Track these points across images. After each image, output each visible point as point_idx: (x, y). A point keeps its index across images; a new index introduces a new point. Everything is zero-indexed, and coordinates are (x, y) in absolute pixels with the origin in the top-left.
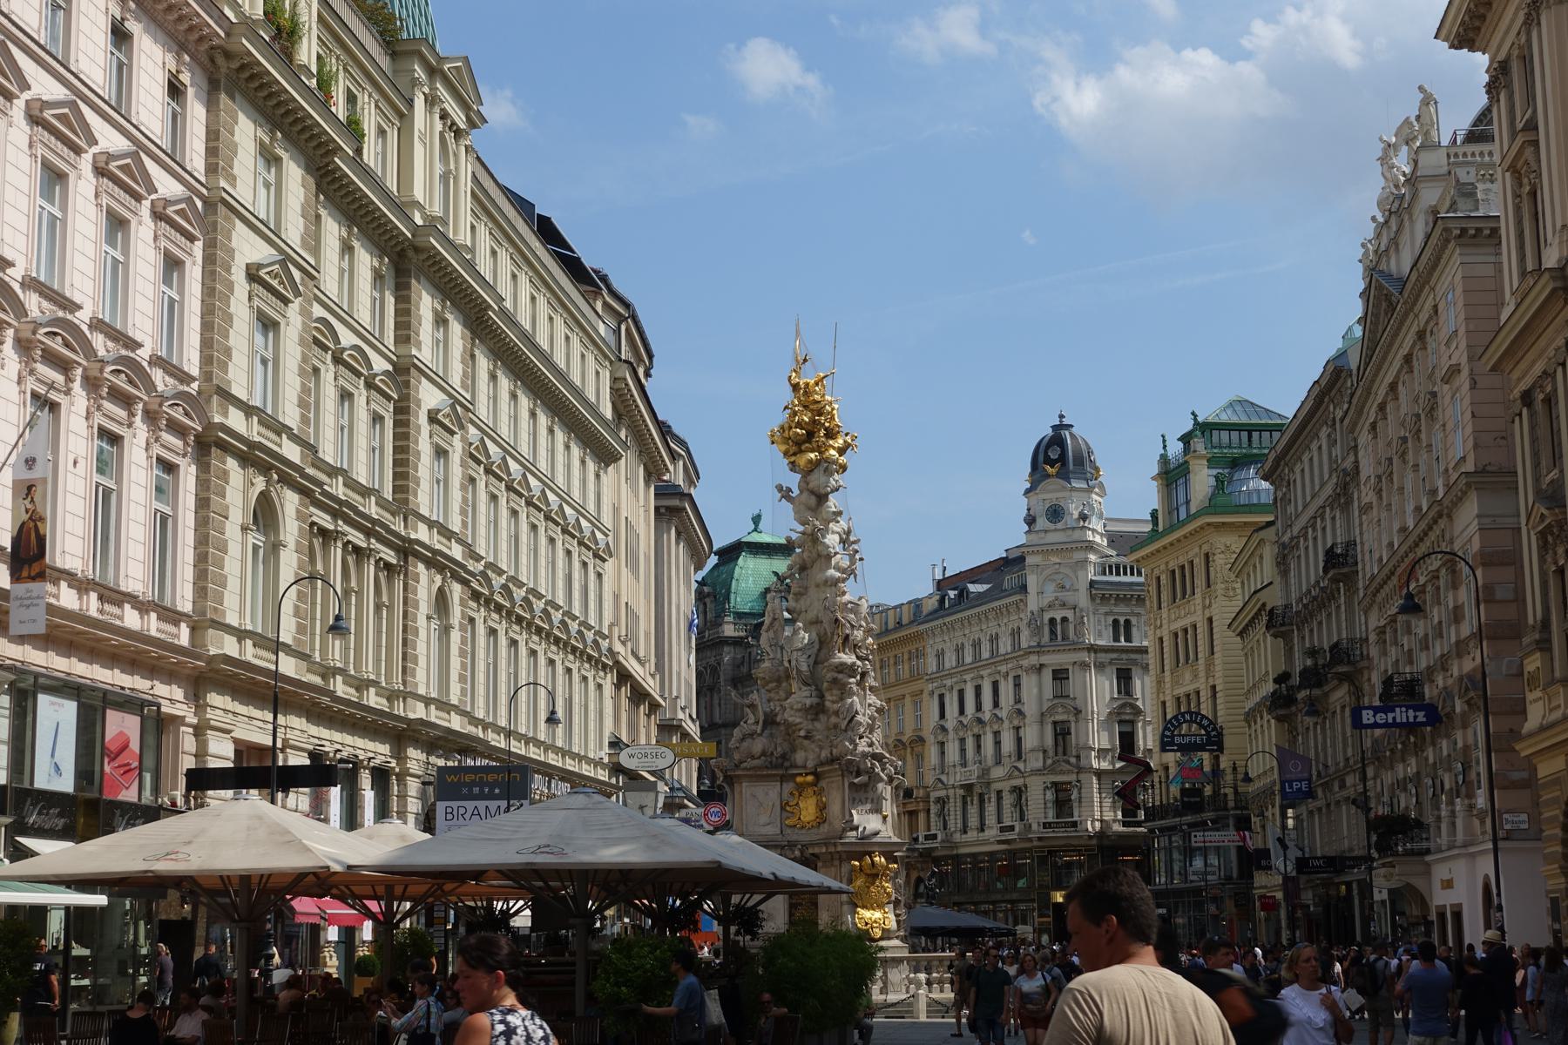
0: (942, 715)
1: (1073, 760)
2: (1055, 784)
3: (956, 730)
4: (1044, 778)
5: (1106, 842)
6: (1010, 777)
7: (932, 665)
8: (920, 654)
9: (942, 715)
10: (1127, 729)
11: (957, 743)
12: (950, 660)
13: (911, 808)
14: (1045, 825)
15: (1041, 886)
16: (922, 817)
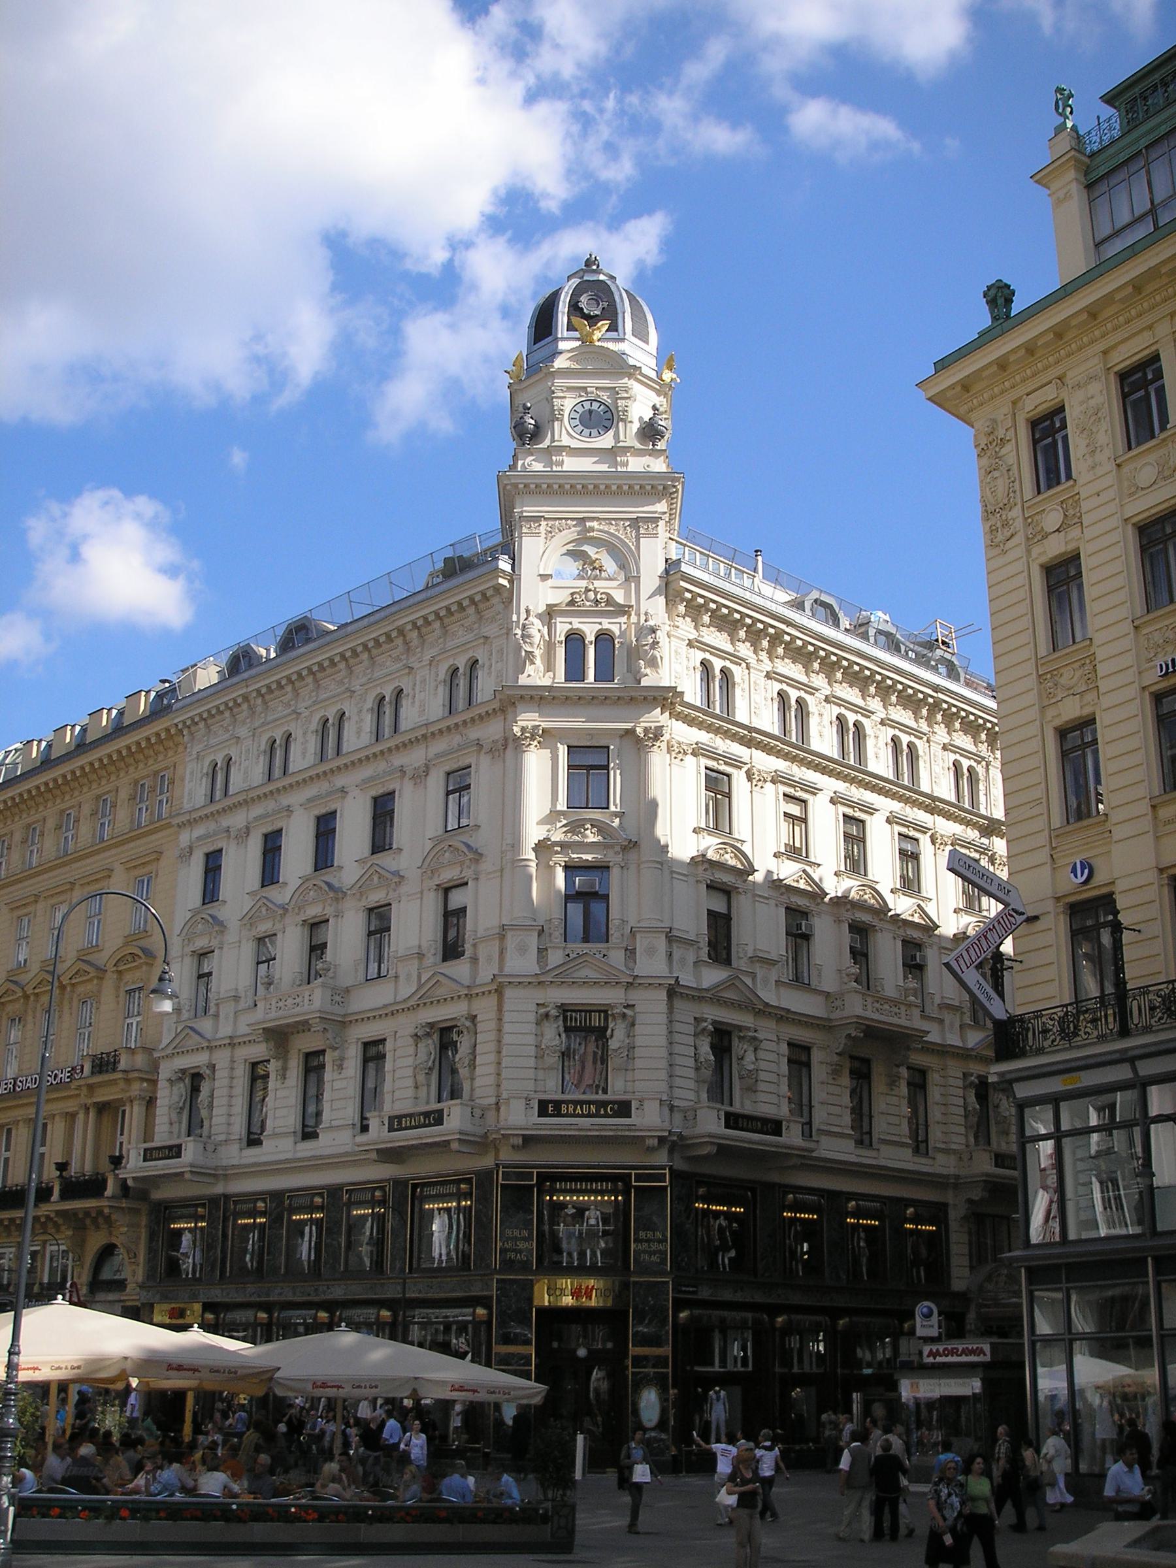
0: (210, 893)
1: (617, 957)
2: (565, 1010)
3: (250, 920)
4: (540, 995)
5: (680, 1165)
6: (424, 1000)
7: (193, 790)
8: (164, 782)
9: (210, 893)
10: (719, 906)
11: (248, 950)
12: (249, 772)
13: (103, 1096)
14: (544, 1108)
15: (508, 1265)
16: (135, 1113)
